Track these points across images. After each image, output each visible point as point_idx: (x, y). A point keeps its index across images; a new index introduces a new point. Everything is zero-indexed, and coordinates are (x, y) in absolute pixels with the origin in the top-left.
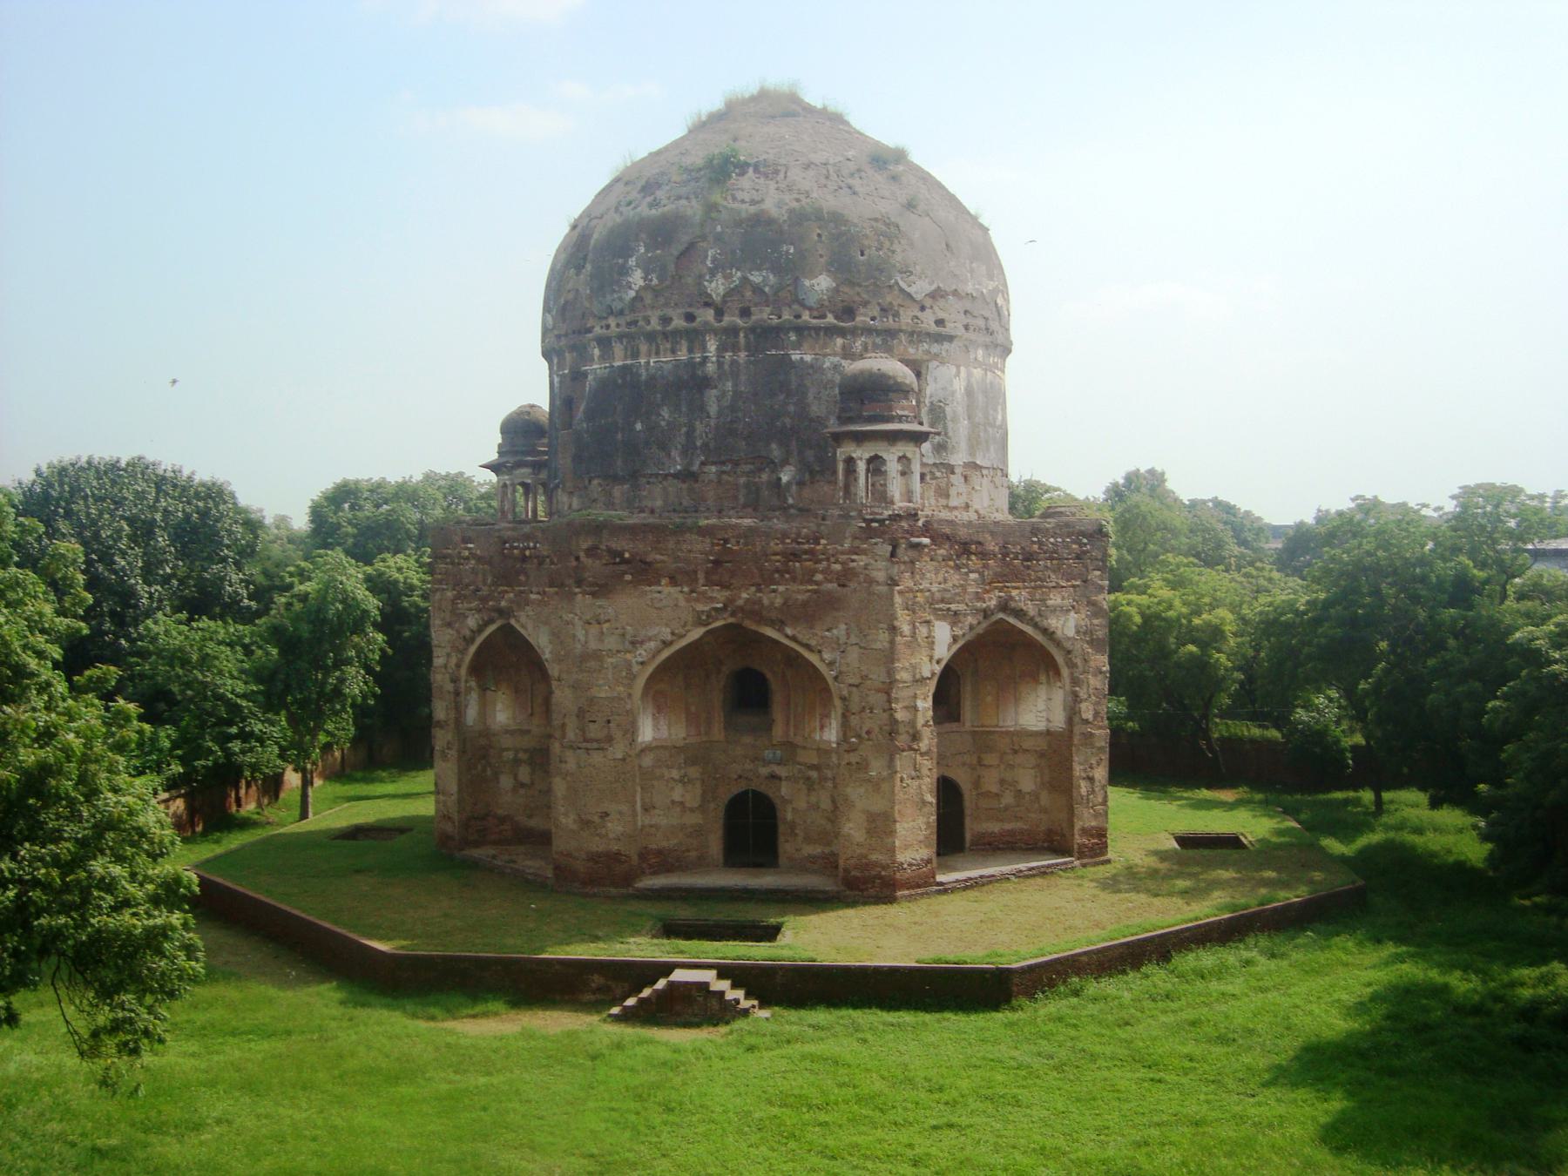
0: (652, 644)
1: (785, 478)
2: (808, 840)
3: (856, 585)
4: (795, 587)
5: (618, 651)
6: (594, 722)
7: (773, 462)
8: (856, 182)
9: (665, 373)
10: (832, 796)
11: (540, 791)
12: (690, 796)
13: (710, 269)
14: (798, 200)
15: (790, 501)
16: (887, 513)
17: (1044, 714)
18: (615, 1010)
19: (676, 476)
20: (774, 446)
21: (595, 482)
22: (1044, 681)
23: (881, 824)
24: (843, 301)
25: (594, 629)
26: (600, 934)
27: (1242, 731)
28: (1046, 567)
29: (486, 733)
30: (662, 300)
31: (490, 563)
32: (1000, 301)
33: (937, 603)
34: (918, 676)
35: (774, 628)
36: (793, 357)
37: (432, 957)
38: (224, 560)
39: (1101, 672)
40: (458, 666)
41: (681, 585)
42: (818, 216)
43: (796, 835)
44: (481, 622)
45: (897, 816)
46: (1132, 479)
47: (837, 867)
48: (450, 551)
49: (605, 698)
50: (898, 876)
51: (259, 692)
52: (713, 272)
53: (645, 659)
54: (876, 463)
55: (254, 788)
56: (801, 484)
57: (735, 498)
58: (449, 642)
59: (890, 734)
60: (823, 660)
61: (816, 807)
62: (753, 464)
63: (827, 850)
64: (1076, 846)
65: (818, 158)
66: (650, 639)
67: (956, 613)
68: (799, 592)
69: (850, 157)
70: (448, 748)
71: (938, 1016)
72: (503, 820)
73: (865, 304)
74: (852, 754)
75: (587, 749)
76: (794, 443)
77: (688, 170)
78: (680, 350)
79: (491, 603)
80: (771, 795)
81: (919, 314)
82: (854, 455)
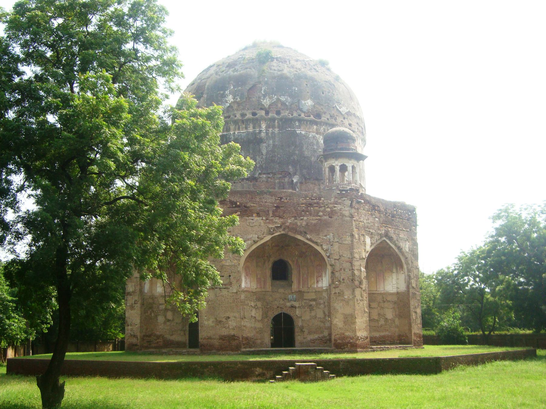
1: (295, 181)
2: (310, 333)
3: (337, 217)
4: (311, 218)
7: (290, 174)
8: (316, 67)
9: (242, 137)
11: (177, 323)
12: (257, 314)
13: (263, 94)
14: (296, 71)
16: (348, 188)
19: (248, 179)
20: (290, 167)
22: (395, 272)
23: (350, 319)
29: (153, 297)
30: (241, 107)
36: (297, 132)
42: (306, 77)
43: (304, 332)
46: (403, 207)
50: (357, 342)
52: (265, 96)
54: (343, 168)
56: (301, 183)
60: (323, 249)
62: (281, 174)
63: (321, 336)
64: (413, 340)
67: (372, 234)
68: (313, 220)
70: (135, 304)
72: (158, 337)
73: (325, 113)
74: (336, 289)
76: (298, 166)
78: (249, 128)
80: (292, 315)
81: (343, 120)
82: (334, 164)
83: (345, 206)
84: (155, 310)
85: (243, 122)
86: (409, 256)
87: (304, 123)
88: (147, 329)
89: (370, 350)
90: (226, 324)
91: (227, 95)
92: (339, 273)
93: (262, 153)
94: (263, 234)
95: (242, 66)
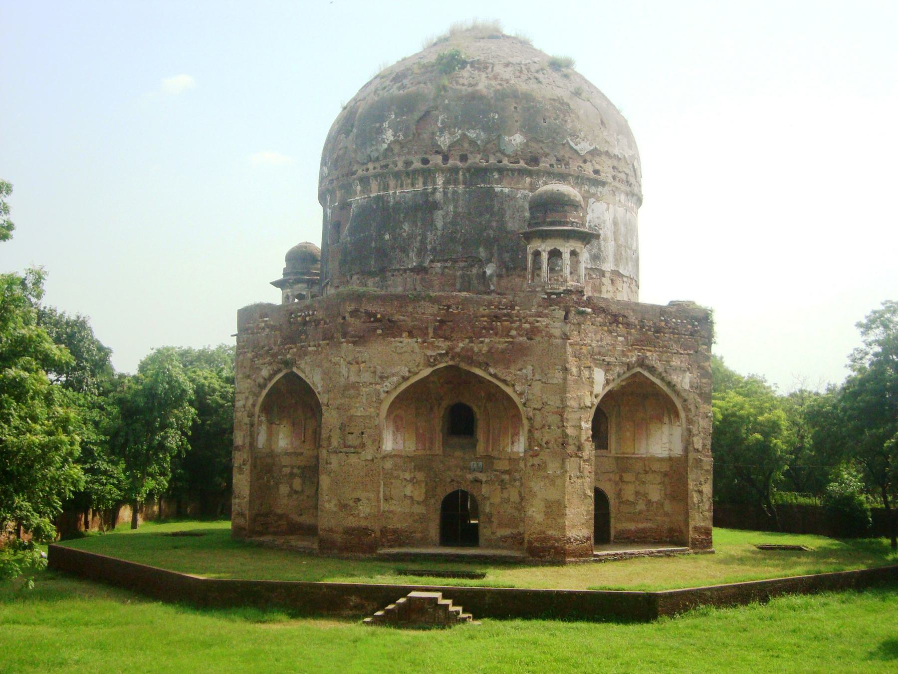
0: (395, 379)
1: (489, 272)
2: (500, 525)
4: (497, 339)
5: (371, 384)
6: (353, 433)
7: (480, 260)
8: (540, 76)
9: (407, 200)
10: (519, 491)
11: (308, 497)
13: (439, 128)
14: (501, 85)
15: (492, 287)
16: (562, 289)
17: (667, 445)
18: (368, 619)
19: (412, 270)
20: (481, 250)
21: (355, 277)
23: (555, 509)
24: (531, 152)
25: (354, 368)
26: (355, 573)
27: (791, 499)
28: (670, 338)
29: (272, 454)
30: (406, 150)
31: (281, 330)
32: (636, 164)
33: (596, 355)
34: (582, 405)
35: (481, 369)
36: (496, 189)
37: (233, 582)
38: (83, 368)
39: (707, 417)
40: (254, 405)
41: (416, 337)
42: (515, 95)
44: (271, 372)
45: (566, 503)
47: (521, 543)
48: (251, 325)
49: (361, 416)
50: (567, 547)
51: (106, 442)
52: (442, 131)
53: (389, 389)
54: (555, 254)
55: (98, 517)
56: (500, 276)
57: (454, 285)
58: (248, 388)
59: (563, 444)
60: (515, 391)
61: (508, 500)
62: (466, 262)
63: (515, 531)
64: (690, 539)
65: (514, 60)
66: (393, 375)
67: (608, 363)
69: (536, 61)
70: (244, 464)
71: (605, 625)
72: (281, 517)
73: (546, 155)
74: (535, 458)
75: (346, 453)
76: (495, 247)
77: (424, 66)
79: (279, 357)
81: (582, 165)
82: (540, 249)
83: (555, 319)
84: (275, 475)
85: (408, 174)
86: (693, 397)
87: (508, 174)
88: (261, 505)
89: (593, 558)
90: (356, 509)
91: (386, 130)
92: (539, 432)
93: (435, 226)
94: (418, 366)
95: (414, 78)
